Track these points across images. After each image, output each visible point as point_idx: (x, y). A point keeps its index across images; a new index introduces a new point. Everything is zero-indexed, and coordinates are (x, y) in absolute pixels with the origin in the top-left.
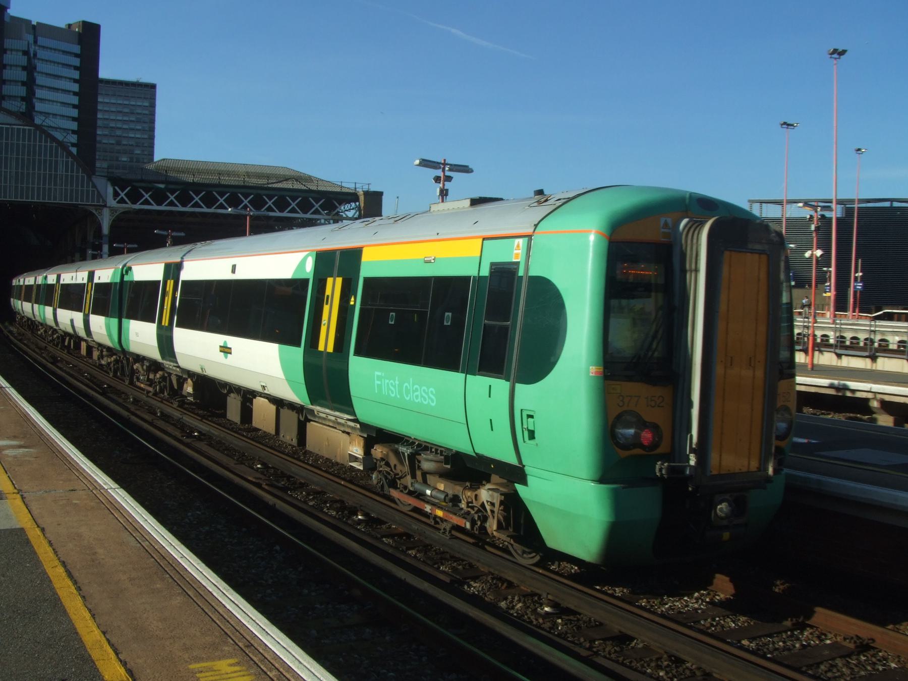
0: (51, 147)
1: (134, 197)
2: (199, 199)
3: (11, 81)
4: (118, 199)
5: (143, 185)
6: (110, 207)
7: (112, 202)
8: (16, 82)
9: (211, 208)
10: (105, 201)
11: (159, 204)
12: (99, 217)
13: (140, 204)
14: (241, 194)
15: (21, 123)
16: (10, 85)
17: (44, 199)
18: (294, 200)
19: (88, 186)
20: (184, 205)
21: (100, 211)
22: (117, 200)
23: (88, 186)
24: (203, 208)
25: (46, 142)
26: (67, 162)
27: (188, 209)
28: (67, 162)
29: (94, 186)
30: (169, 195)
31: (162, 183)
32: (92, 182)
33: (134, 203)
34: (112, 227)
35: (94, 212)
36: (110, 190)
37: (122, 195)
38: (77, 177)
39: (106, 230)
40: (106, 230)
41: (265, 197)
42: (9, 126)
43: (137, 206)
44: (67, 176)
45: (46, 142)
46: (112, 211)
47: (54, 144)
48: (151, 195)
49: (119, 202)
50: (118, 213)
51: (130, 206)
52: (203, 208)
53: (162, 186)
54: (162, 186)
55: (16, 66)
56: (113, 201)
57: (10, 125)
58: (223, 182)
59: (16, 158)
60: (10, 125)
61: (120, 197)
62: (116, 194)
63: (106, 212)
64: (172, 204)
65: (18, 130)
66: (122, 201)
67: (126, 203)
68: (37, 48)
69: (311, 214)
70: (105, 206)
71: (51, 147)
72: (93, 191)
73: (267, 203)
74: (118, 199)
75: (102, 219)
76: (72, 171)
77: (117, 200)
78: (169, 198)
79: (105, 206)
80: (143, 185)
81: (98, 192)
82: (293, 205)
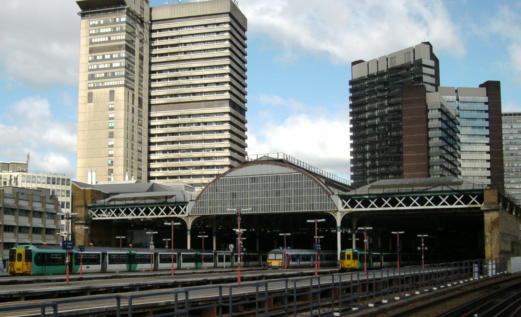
0: (310, 182)
2: (385, 202)
3: (432, 128)
4: (344, 206)
5: (357, 197)
6: (340, 211)
7: (341, 208)
8: (435, 128)
10: (337, 208)
12: (335, 217)
15: (296, 172)
16: (432, 131)
18: (459, 197)
19: (329, 201)
23: (329, 201)
25: (308, 180)
29: (332, 200)
30: (358, 202)
31: (367, 195)
32: (331, 199)
33: (353, 207)
35: (333, 214)
36: (340, 202)
37: (346, 204)
39: (339, 224)
40: (339, 224)
42: (290, 174)
43: (355, 209)
45: (308, 180)
47: (312, 181)
49: (345, 208)
50: (345, 214)
53: (367, 197)
54: (367, 197)
55: (435, 119)
57: (291, 173)
58: (414, 191)
60: (291, 173)
61: (345, 205)
62: (344, 204)
63: (338, 214)
64: (373, 206)
65: (295, 175)
66: (346, 207)
67: (349, 208)
68: (459, 103)
70: (338, 211)
71: (310, 182)
72: (331, 203)
75: (337, 218)
79: (338, 211)
80: (357, 197)
81: (334, 203)
82: (444, 200)
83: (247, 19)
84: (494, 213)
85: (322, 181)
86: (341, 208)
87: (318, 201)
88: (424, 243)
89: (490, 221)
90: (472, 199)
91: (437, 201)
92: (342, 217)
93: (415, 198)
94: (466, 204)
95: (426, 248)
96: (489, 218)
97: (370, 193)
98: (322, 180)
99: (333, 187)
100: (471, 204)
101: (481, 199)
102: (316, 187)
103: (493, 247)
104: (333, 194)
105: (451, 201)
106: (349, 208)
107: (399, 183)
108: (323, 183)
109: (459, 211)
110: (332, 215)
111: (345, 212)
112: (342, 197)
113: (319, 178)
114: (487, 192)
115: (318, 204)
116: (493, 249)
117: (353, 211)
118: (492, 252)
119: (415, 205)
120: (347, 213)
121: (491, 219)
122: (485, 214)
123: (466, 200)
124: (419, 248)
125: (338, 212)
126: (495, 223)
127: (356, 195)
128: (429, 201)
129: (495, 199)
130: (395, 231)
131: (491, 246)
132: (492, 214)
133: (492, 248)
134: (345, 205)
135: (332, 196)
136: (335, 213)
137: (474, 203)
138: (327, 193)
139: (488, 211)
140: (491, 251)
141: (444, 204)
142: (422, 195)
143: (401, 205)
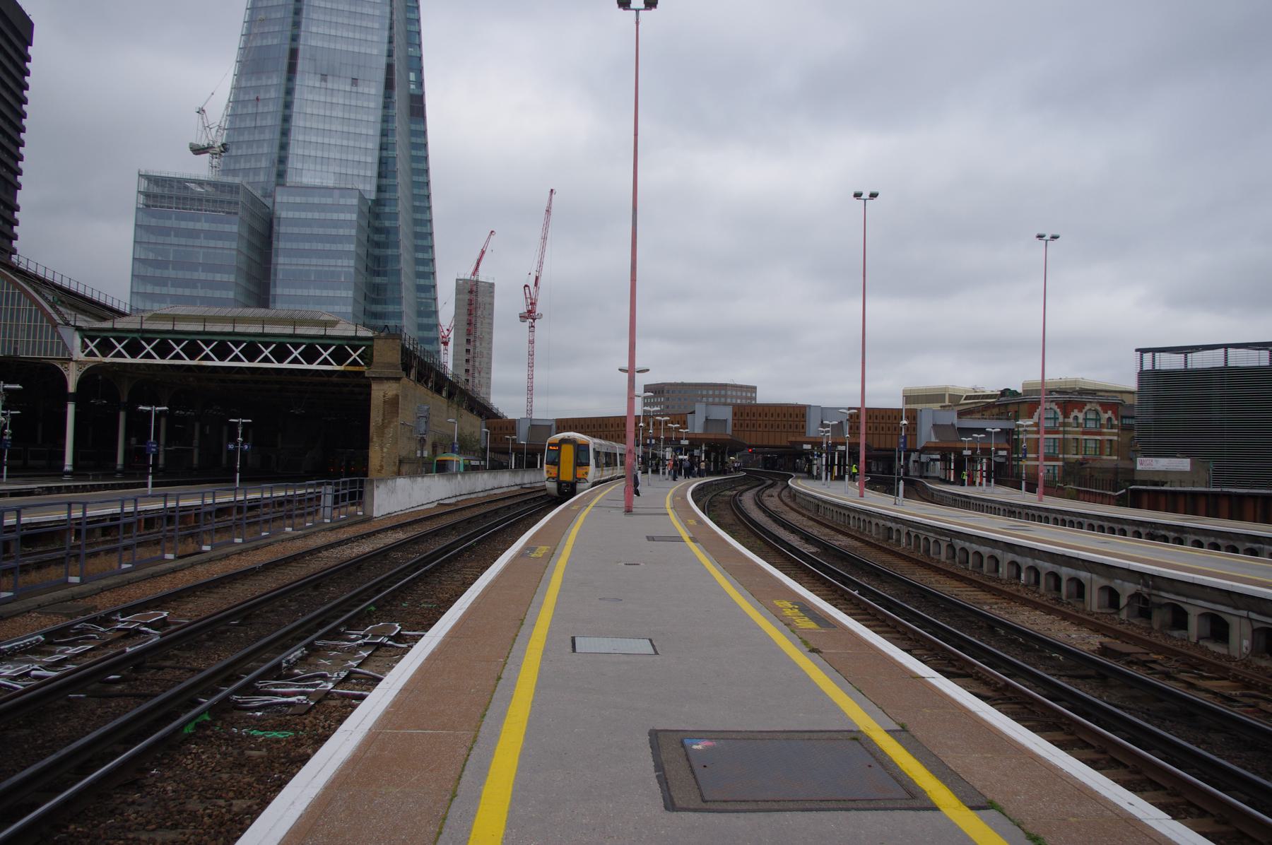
0: (14, 294)
1: (105, 347)
4: (87, 351)
6: (76, 361)
7: (78, 355)
9: (224, 361)
11: (222, 359)
12: (65, 372)
13: (111, 357)
14: (114, 338)
17: (39, 354)
19: (53, 338)
20: (251, 360)
21: (66, 366)
22: (85, 353)
23: (53, 338)
24: (155, 358)
25: (8, 288)
26: (31, 310)
27: (226, 363)
28: (31, 310)
29: (60, 337)
33: (105, 355)
34: (81, 383)
35: (59, 366)
37: (92, 346)
38: (41, 327)
39: (72, 388)
40: (72, 388)
41: (260, 345)
43: (108, 360)
44: (29, 327)
45: (8, 288)
46: (80, 366)
48: (99, 343)
49: (86, 355)
50: (87, 367)
51: (100, 358)
52: (155, 358)
53: (135, 335)
54: (135, 335)
56: (81, 354)
59: (11, 308)
61: (89, 349)
62: (85, 346)
63: (72, 366)
64: (148, 356)
66: (91, 354)
67: (96, 356)
69: (259, 362)
70: (71, 360)
71: (14, 294)
73: (208, 347)
74: (87, 351)
75: (68, 375)
76: (36, 321)
77: (85, 353)
78: (263, 352)
79: (71, 360)
81: (65, 345)
82: (296, 353)
83: (32, 25)
84: (390, 385)
85: (46, 295)
86: (78, 355)
87: (28, 336)
88: (10, 428)
89: (382, 399)
90: (352, 355)
91: (281, 354)
92: (81, 373)
93: (237, 344)
94: (340, 364)
95: (246, 447)
96: (380, 393)
97: (145, 326)
98: (46, 292)
99: (66, 307)
100: (348, 365)
101: (367, 357)
102: (25, 304)
103: (385, 450)
104: (67, 324)
105: (310, 355)
106: (96, 356)
107: (212, 314)
108: (46, 299)
109: (334, 379)
110: (59, 368)
111: (86, 362)
112: (87, 334)
113: (40, 288)
114: (380, 342)
115: (28, 342)
116: (384, 455)
117: (105, 363)
118: (382, 461)
119: (237, 358)
120: (91, 365)
121: (384, 396)
122: (374, 387)
123: (340, 356)
124: (231, 447)
125: (71, 363)
126: (393, 405)
127: (114, 330)
128: (266, 352)
129: (396, 357)
130: (146, 405)
131: (382, 450)
132: (387, 386)
133: (383, 452)
134: (89, 349)
135: (60, 329)
136: (66, 363)
137: (355, 363)
138: (51, 319)
139: (380, 379)
140: (380, 458)
141: (295, 361)
142: (253, 339)
143: (207, 357)
